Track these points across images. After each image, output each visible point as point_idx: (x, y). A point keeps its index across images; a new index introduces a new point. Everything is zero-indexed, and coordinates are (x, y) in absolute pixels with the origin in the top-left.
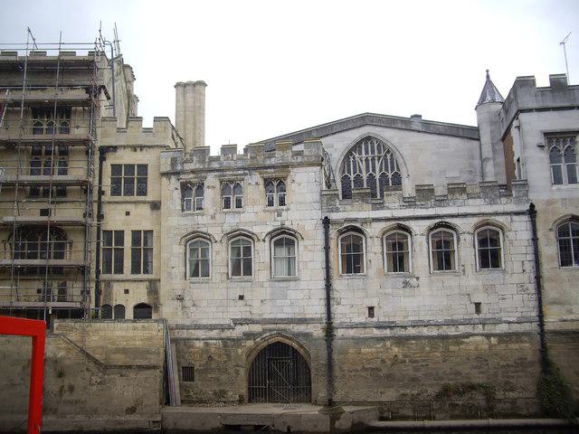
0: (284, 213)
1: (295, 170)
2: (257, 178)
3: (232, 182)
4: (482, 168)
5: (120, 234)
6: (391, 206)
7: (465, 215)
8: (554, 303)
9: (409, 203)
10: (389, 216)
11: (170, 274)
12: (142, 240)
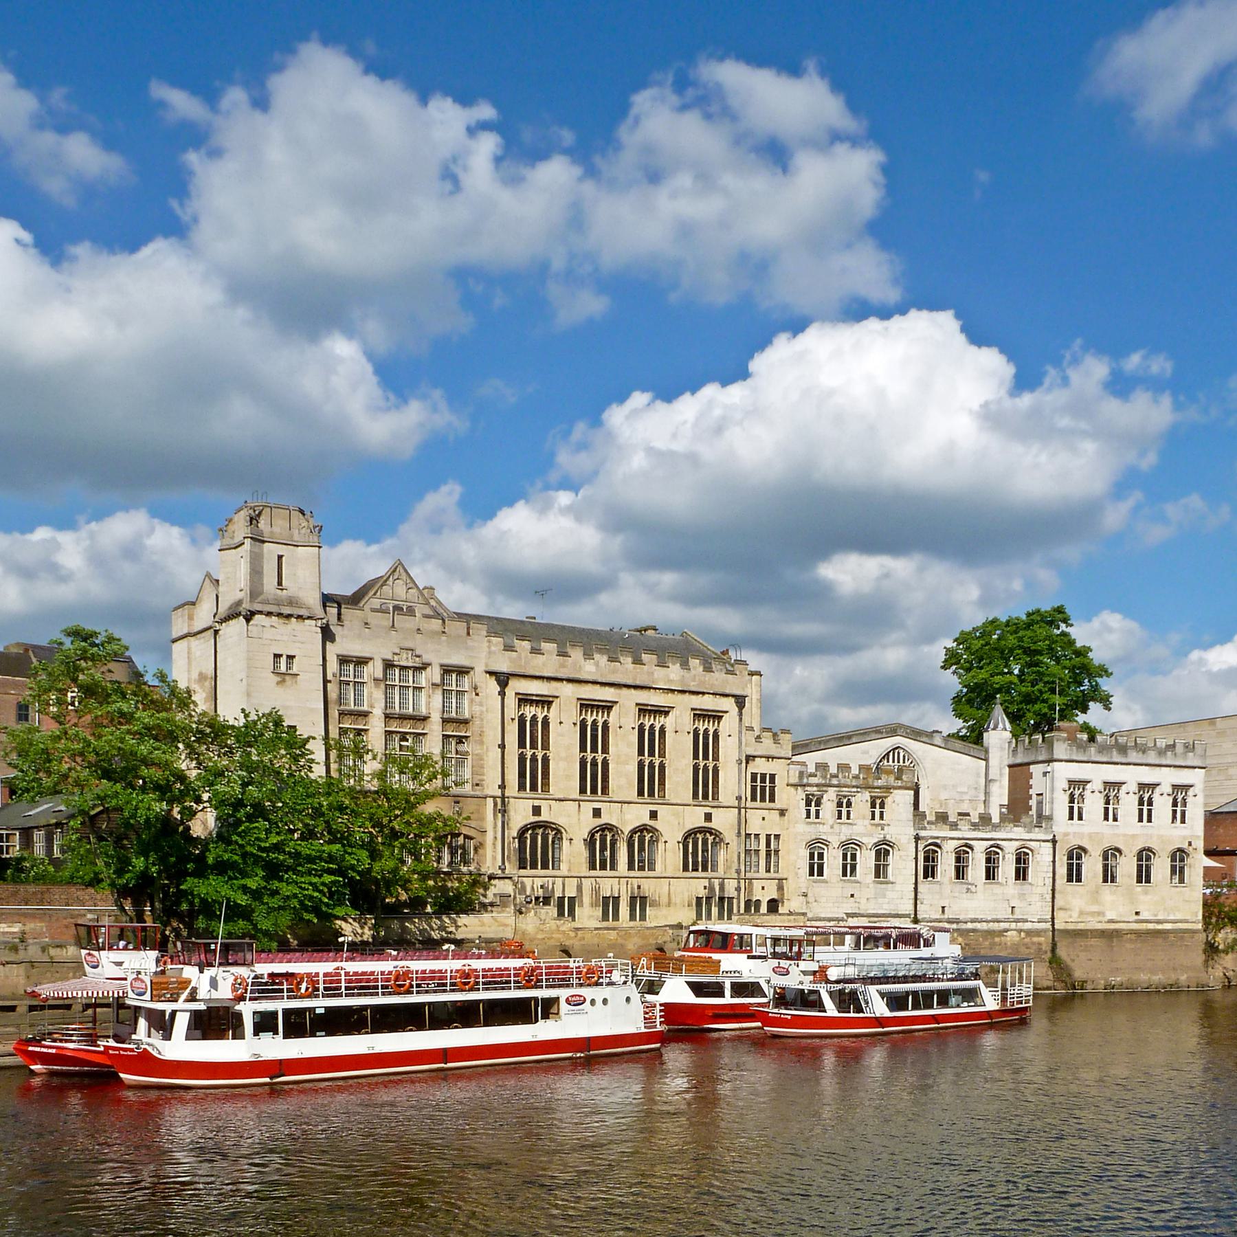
0: (886, 828)
1: (896, 791)
2: (866, 795)
3: (845, 797)
4: (986, 786)
5: (757, 836)
6: (963, 828)
7: (1011, 840)
8: (1061, 909)
9: (975, 826)
10: (961, 836)
11: (797, 874)
12: (772, 840)
